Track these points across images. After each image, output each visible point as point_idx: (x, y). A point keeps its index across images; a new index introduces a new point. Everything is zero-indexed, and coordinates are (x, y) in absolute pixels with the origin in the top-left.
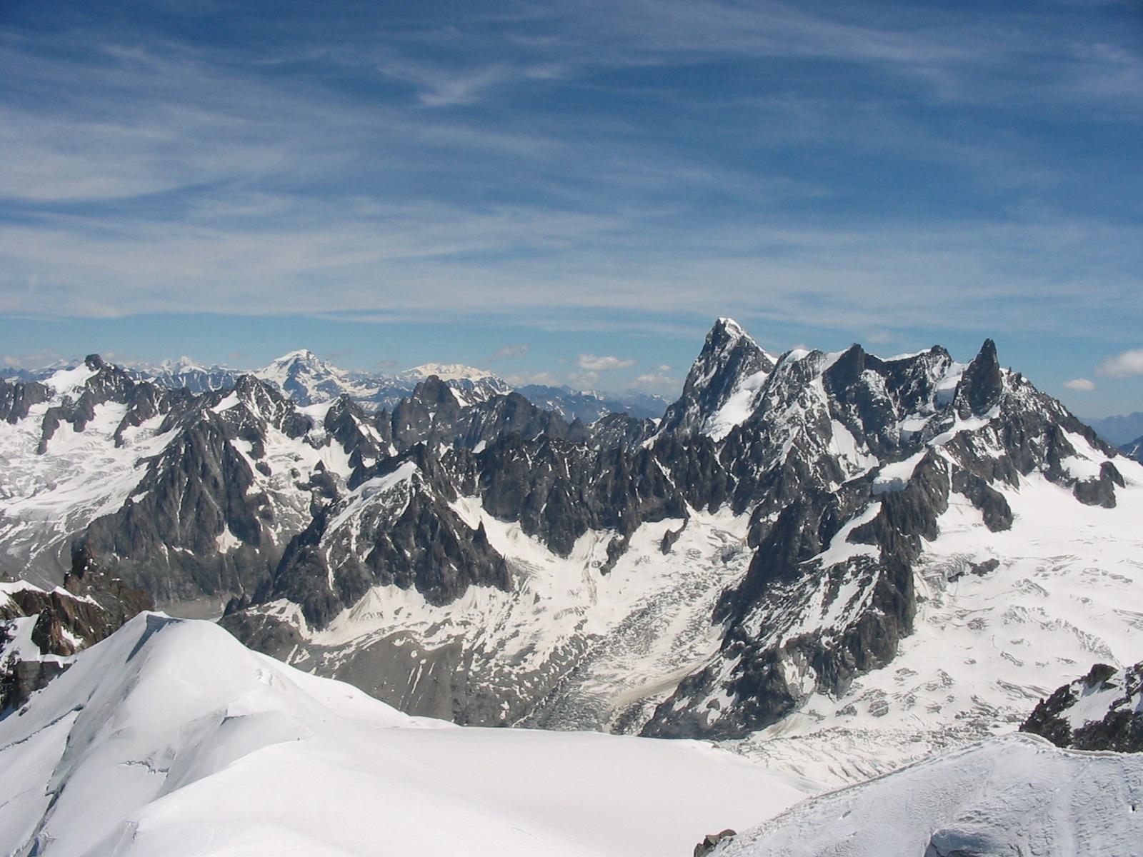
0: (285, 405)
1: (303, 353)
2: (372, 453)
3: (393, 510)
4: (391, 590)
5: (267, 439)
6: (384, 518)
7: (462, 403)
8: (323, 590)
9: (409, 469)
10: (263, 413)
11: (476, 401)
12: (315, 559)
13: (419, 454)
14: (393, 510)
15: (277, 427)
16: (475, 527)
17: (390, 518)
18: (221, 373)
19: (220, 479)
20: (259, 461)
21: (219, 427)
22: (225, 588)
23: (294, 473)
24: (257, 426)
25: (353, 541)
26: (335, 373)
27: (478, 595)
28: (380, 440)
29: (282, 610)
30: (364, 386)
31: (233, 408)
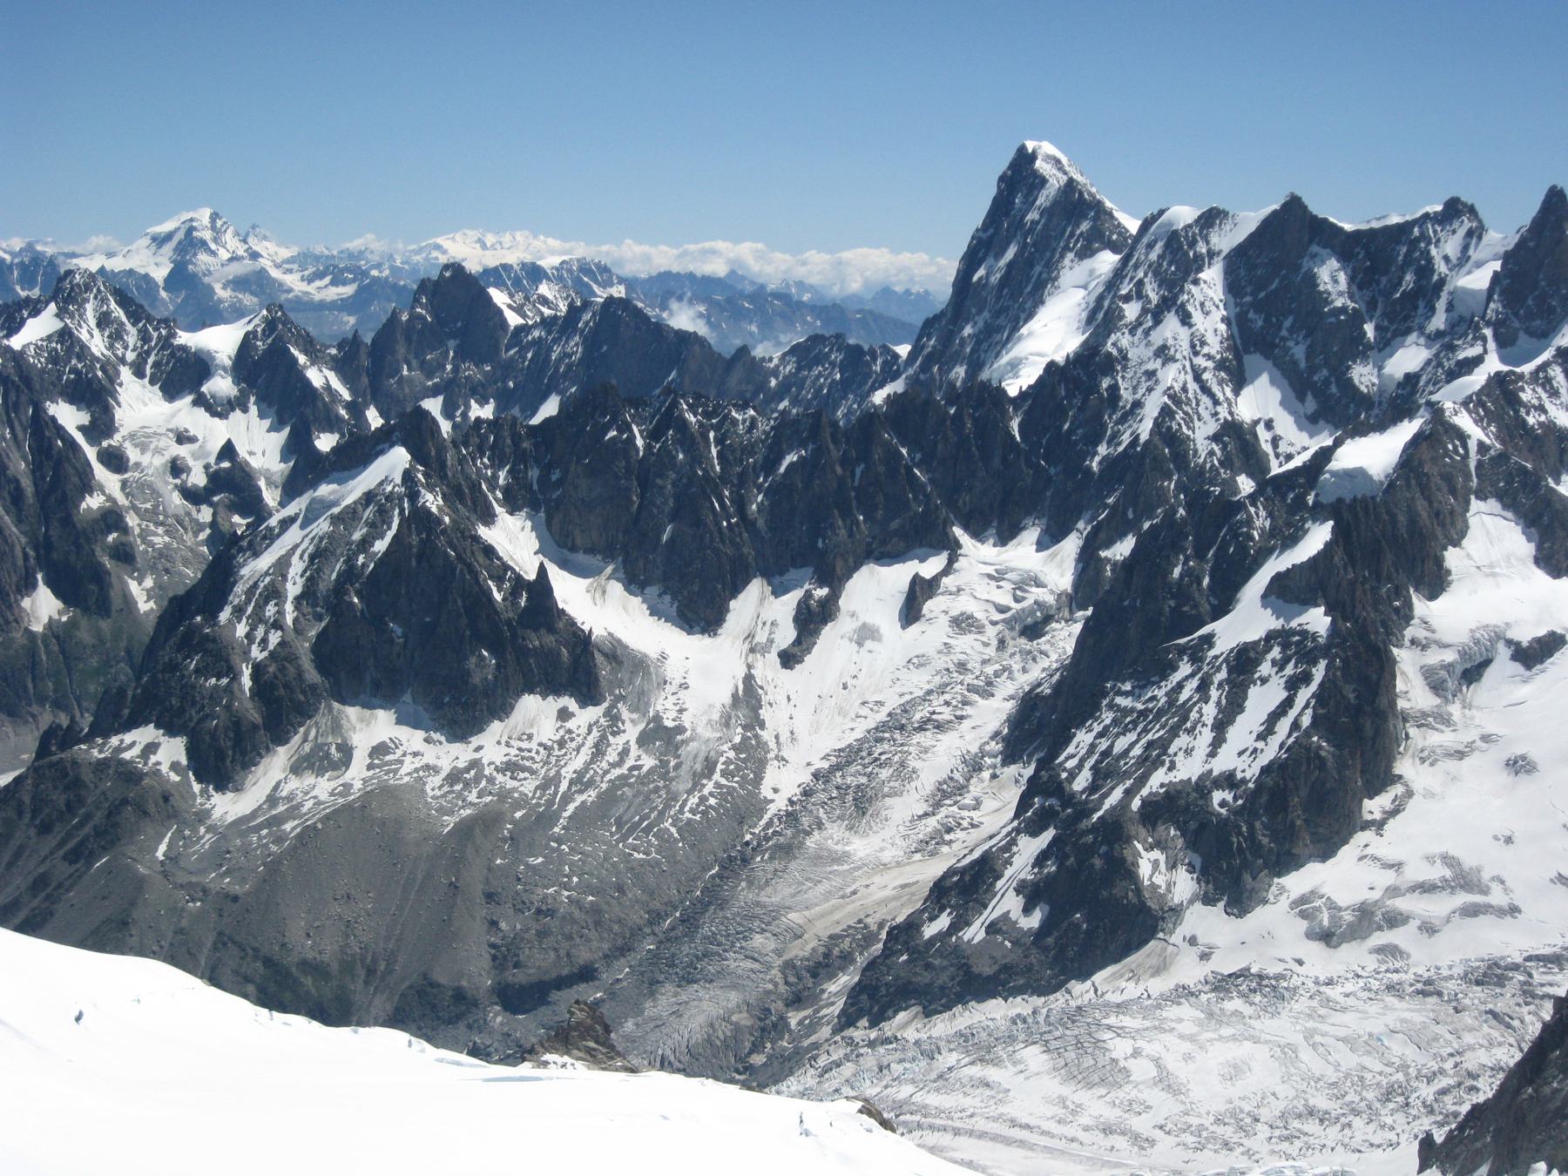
0: (156, 329)
1: (204, 216)
2: (331, 424)
3: (365, 544)
4: (872, 573)
5: (121, 399)
6: (350, 561)
7: (513, 320)
8: (228, 707)
9: (398, 458)
10: (111, 347)
11: (542, 314)
12: (210, 646)
13: (411, 429)
14: (365, 544)
15: (139, 374)
16: (531, 576)
17: (361, 559)
18: (37, 259)
19: (27, 484)
20: (105, 444)
21: (20, 378)
22: (42, 700)
23: (176, 468)
24: (100, 373)
25: (289, 607)
26: (272, 254)
27: (537, 713)
28: (346, 395)
29: (151, 748)
30: (327, 280)
31: (49, 338)
